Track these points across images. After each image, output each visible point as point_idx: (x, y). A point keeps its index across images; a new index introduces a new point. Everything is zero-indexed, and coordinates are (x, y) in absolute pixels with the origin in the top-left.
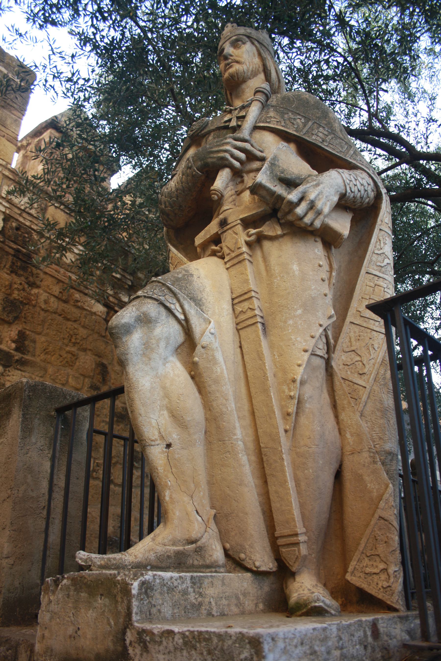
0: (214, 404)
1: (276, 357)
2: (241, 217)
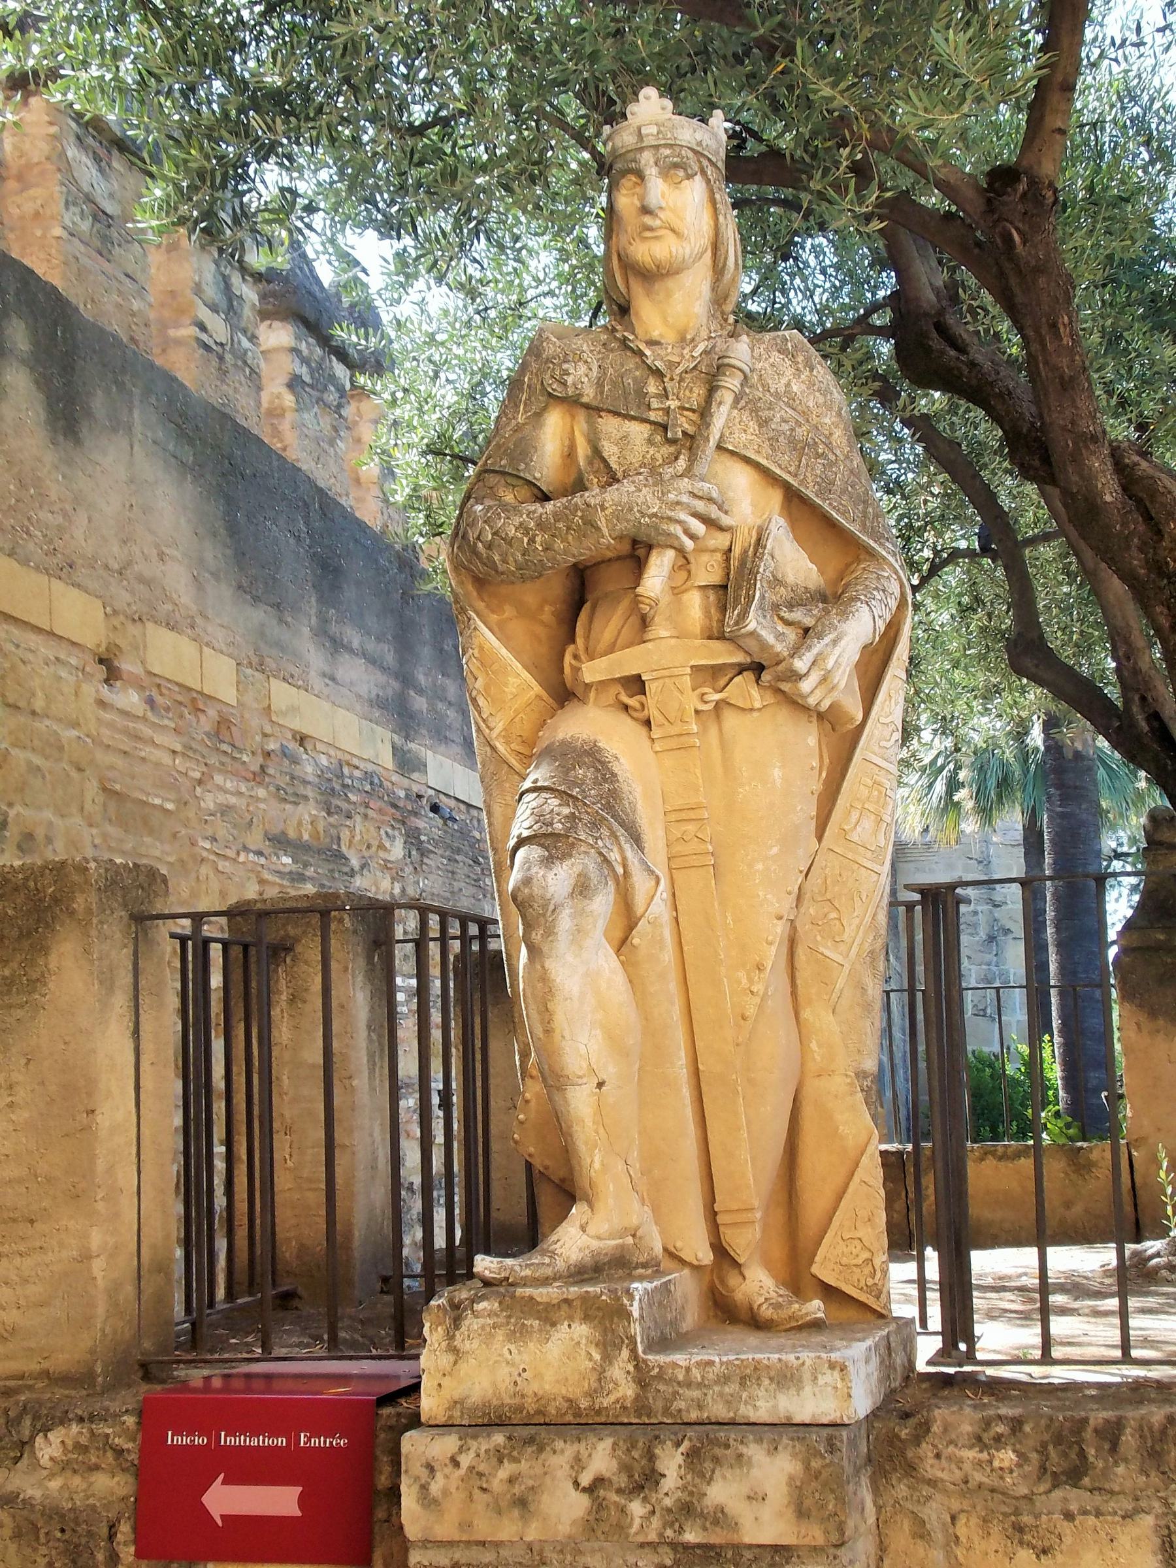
1: (729, 920)
2: (693, 663)
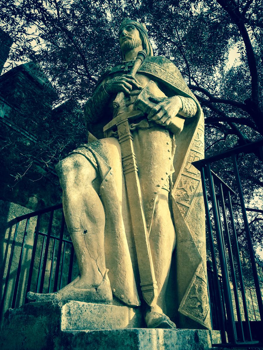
0: (111, 211)
1: (144, 189)
2: (128, 117)
